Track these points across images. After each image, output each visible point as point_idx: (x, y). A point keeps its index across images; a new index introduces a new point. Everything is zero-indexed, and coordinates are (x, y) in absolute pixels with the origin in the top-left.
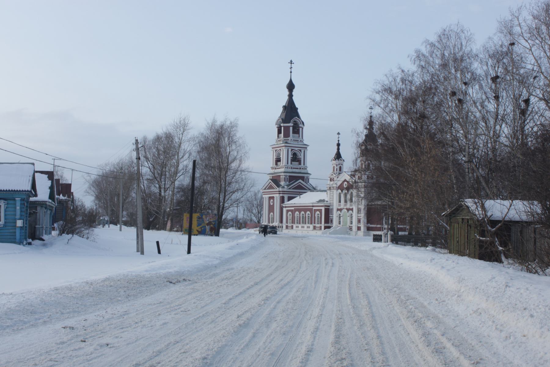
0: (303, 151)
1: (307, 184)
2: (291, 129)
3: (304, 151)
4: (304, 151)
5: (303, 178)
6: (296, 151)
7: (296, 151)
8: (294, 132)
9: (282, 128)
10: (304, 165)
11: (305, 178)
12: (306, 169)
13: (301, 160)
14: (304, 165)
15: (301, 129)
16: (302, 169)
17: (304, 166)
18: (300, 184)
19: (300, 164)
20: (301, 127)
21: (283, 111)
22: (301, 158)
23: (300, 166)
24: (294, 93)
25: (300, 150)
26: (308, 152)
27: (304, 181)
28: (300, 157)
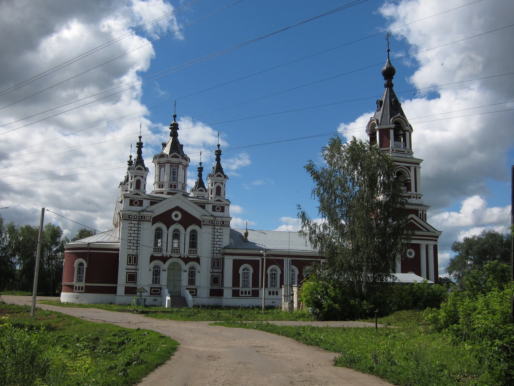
0: (412, 169)
1: (423, 220)
2: (392, 132)
3: (415, 169)
4: (415, 169)
5: (416, 212)
6: (401, 168)
7: (401, 168)
8: (397, 138)
9: (378, 133)
10: (416, 191)
11: (420, 212)
12: (420, 198)
13: (410, 183)
14: (416, 191)
15: (407, 134)
16: (414, 197)
17: (416, 193)
18: (412, 220)
19: (409, 189)
20: (408, 131)
21: (378, 109)
22: (410, 180)
23: (409, 192)
24: (393, 81)
25: (409, 168)
26: (421, 170)
27: (418, 217)
28: (409, 178)
